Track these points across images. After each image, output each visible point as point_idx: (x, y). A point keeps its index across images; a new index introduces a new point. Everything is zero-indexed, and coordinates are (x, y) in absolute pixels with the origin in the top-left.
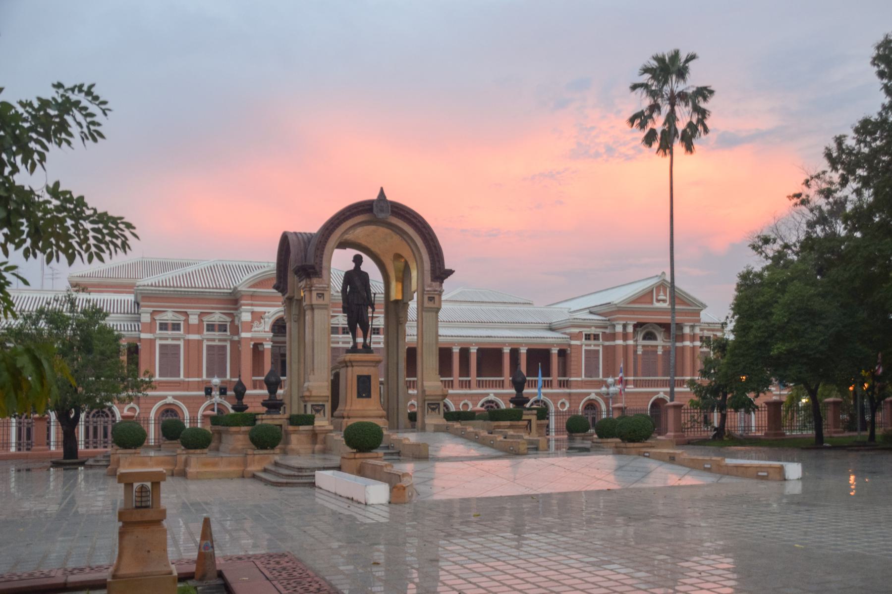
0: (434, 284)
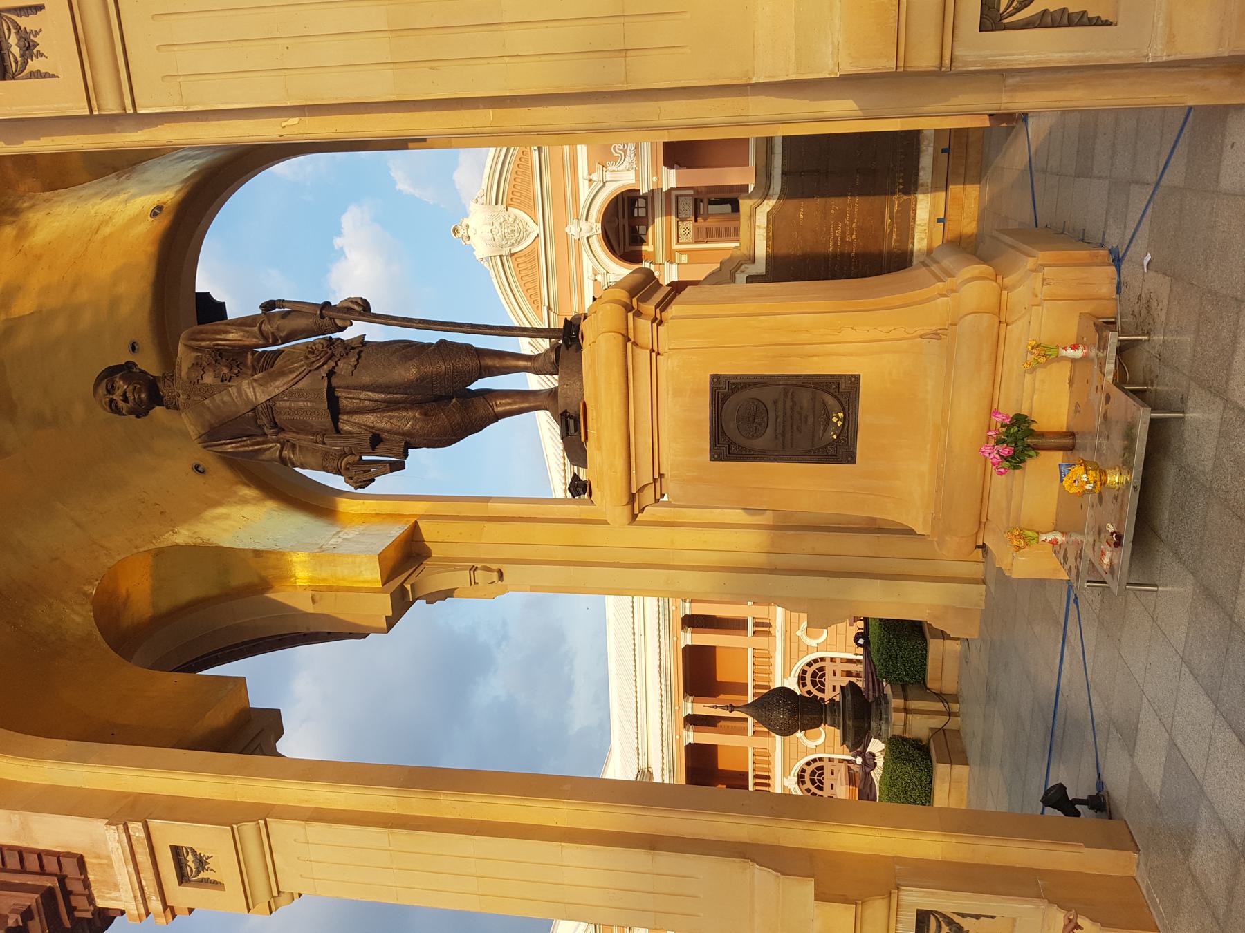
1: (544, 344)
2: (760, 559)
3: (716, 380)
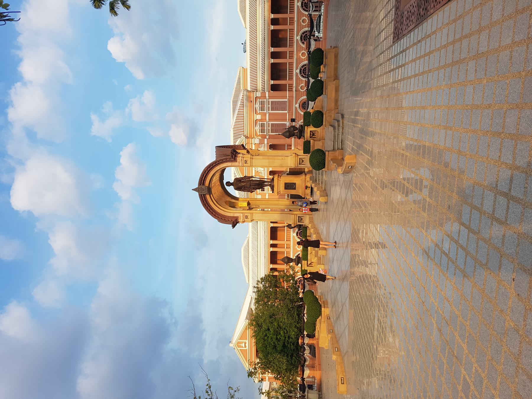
1: (270, 180)
2: (288, 204)
3: (285, 183)
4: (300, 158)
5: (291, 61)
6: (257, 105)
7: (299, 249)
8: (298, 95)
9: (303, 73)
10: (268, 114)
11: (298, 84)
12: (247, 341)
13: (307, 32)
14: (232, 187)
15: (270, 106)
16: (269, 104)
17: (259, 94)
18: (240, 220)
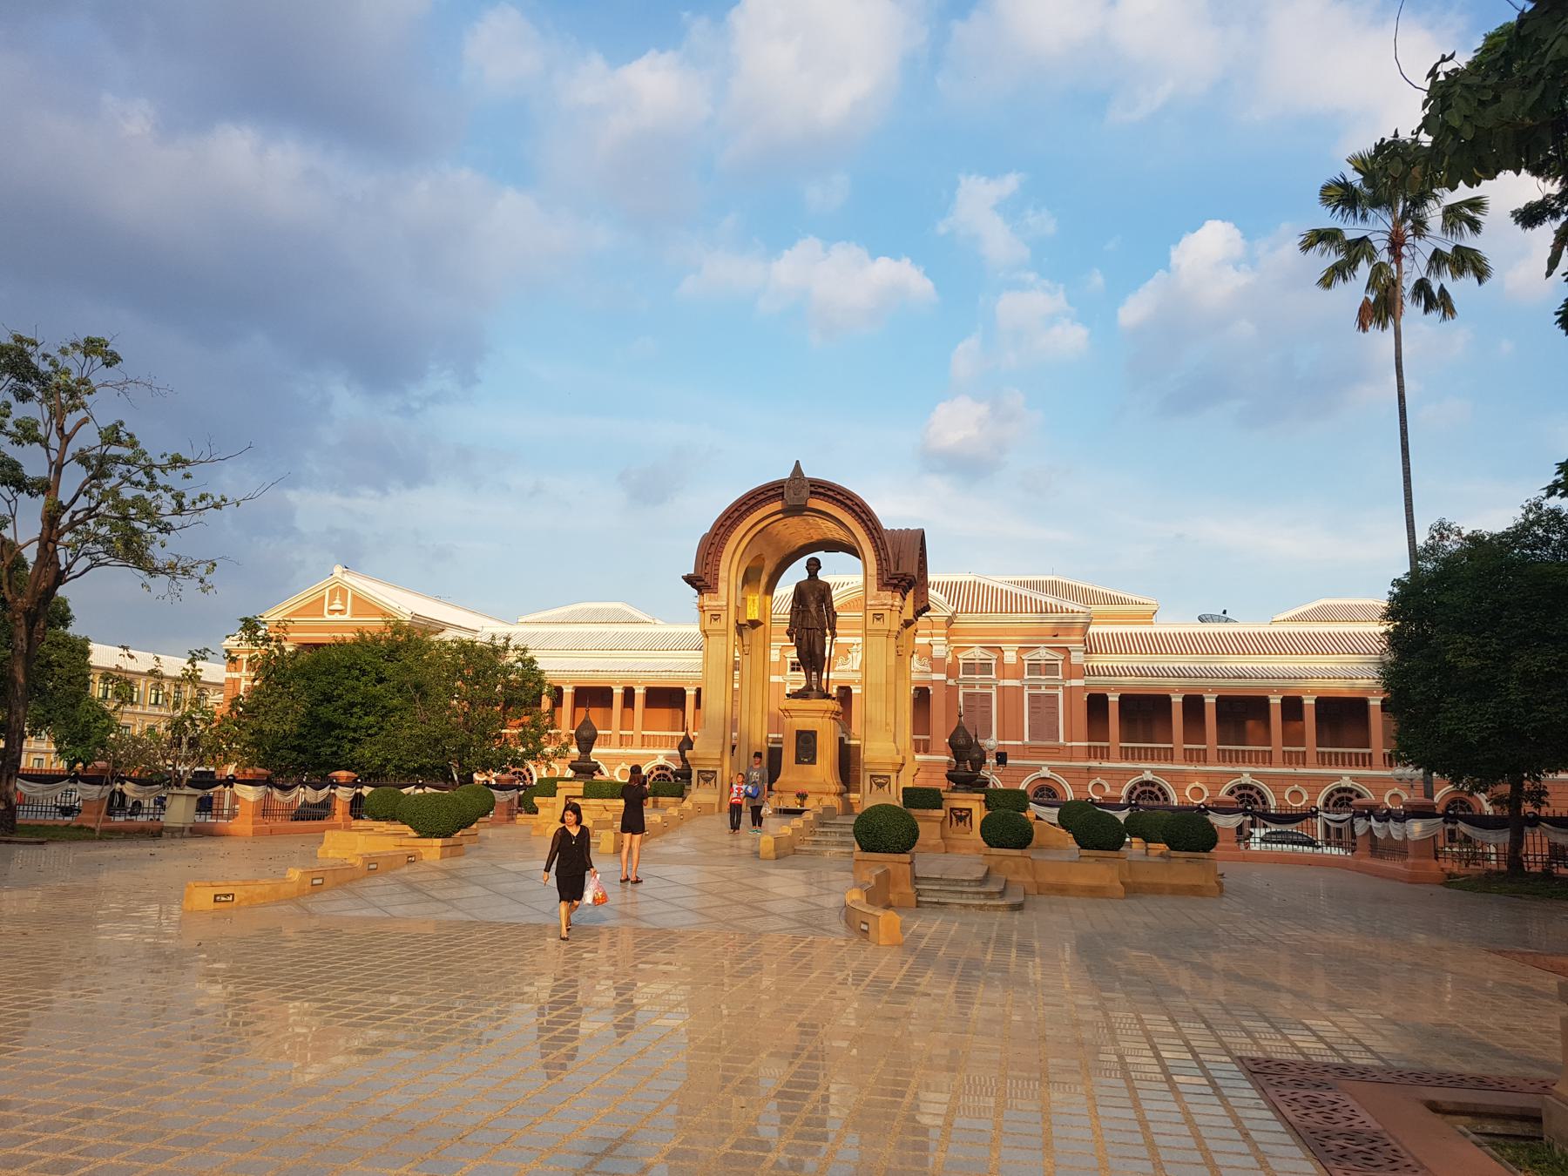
0: (882, 594)
1: (824, 687)
2: (752, 741)
4: (889, 777)
5: (1178, 754)
6: (1045, 651)
7: (616, 774)
8: (1076, 775)
9: (1144, 792)
10: (1019, 685)
11: (1109, 776)
12: (346, 617)
13: (1264, 803)
14: (805, 576)
15: (1043, 691)
16: (1048, 687)
17: (1077, 658)
18: (708, 600)
